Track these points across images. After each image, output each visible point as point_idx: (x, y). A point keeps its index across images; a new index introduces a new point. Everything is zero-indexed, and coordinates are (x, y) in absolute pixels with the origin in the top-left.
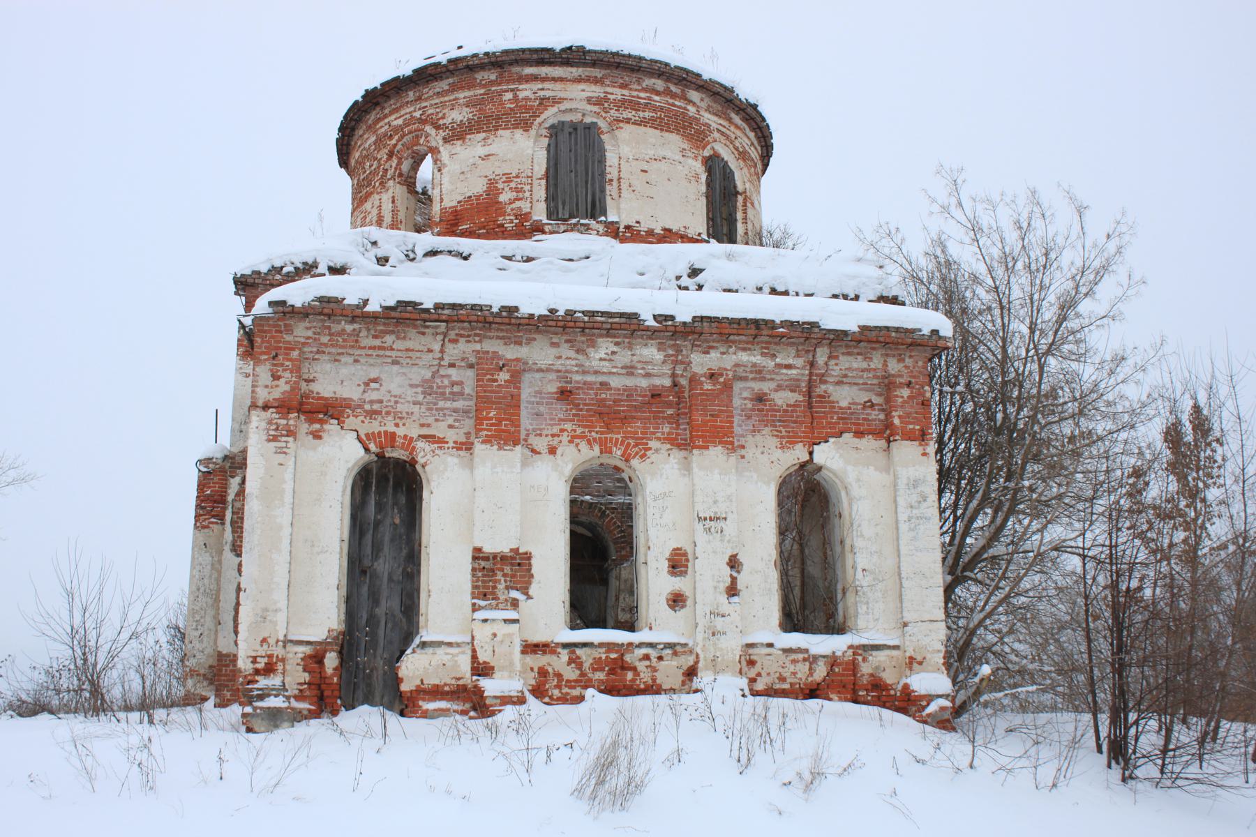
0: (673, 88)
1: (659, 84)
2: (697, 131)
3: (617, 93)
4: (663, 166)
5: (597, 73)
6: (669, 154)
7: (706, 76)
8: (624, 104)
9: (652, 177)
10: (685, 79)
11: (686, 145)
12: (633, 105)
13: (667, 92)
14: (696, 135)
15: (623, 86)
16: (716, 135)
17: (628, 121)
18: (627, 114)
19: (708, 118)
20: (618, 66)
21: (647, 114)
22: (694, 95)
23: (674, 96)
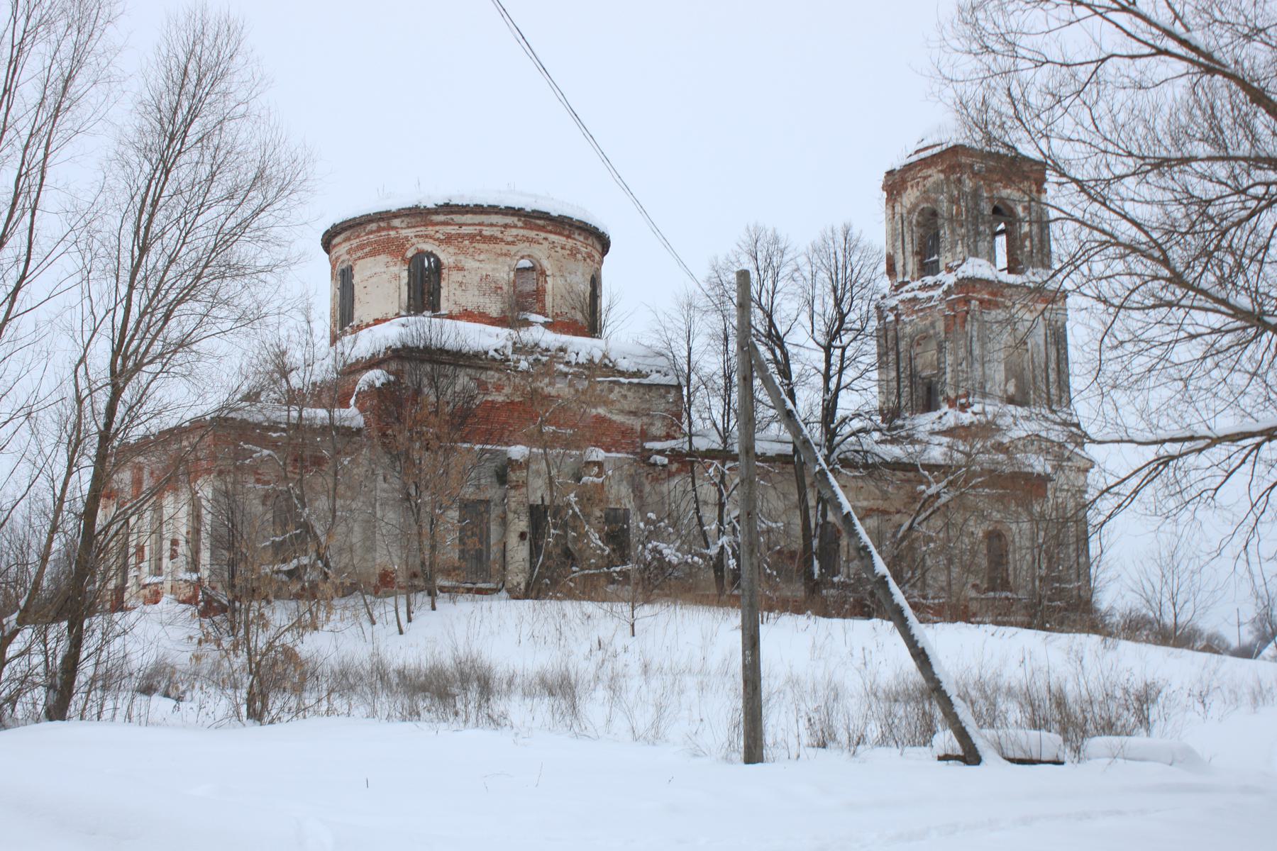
0: (382, 224)
1: (374, 226)
2: (398, 246)
3: (355, 242)
4: (374, 279)
5: (348, 233)
6: (378, 270)
7: (394, 209)
8: (361, 247)
9: (369, 289)
10: (384, 218)
11: (389, 259)
12: (361, 247)
13: (379, 229)
14: (394, 248)
15: (358, 236)
16: (414, 240)
17: (359, 258)
18: (359, 254)
19: (404, 233)
20: (351, 227)
21: (367, 250)
22: (396, 222)
23: (384, 229)
